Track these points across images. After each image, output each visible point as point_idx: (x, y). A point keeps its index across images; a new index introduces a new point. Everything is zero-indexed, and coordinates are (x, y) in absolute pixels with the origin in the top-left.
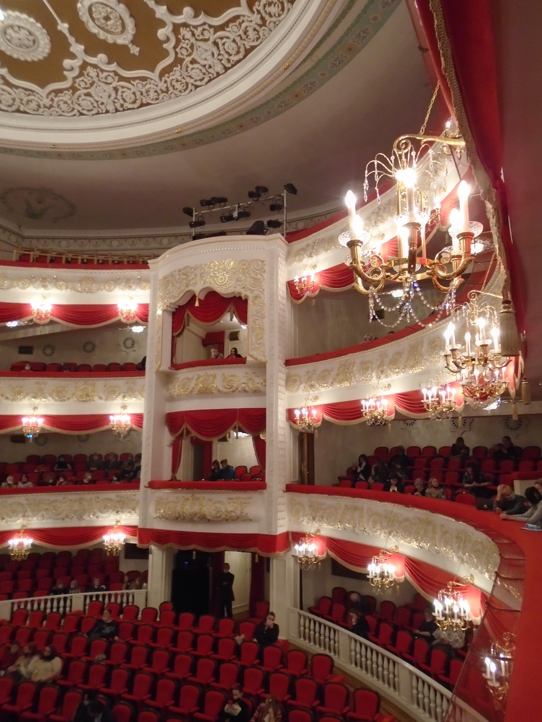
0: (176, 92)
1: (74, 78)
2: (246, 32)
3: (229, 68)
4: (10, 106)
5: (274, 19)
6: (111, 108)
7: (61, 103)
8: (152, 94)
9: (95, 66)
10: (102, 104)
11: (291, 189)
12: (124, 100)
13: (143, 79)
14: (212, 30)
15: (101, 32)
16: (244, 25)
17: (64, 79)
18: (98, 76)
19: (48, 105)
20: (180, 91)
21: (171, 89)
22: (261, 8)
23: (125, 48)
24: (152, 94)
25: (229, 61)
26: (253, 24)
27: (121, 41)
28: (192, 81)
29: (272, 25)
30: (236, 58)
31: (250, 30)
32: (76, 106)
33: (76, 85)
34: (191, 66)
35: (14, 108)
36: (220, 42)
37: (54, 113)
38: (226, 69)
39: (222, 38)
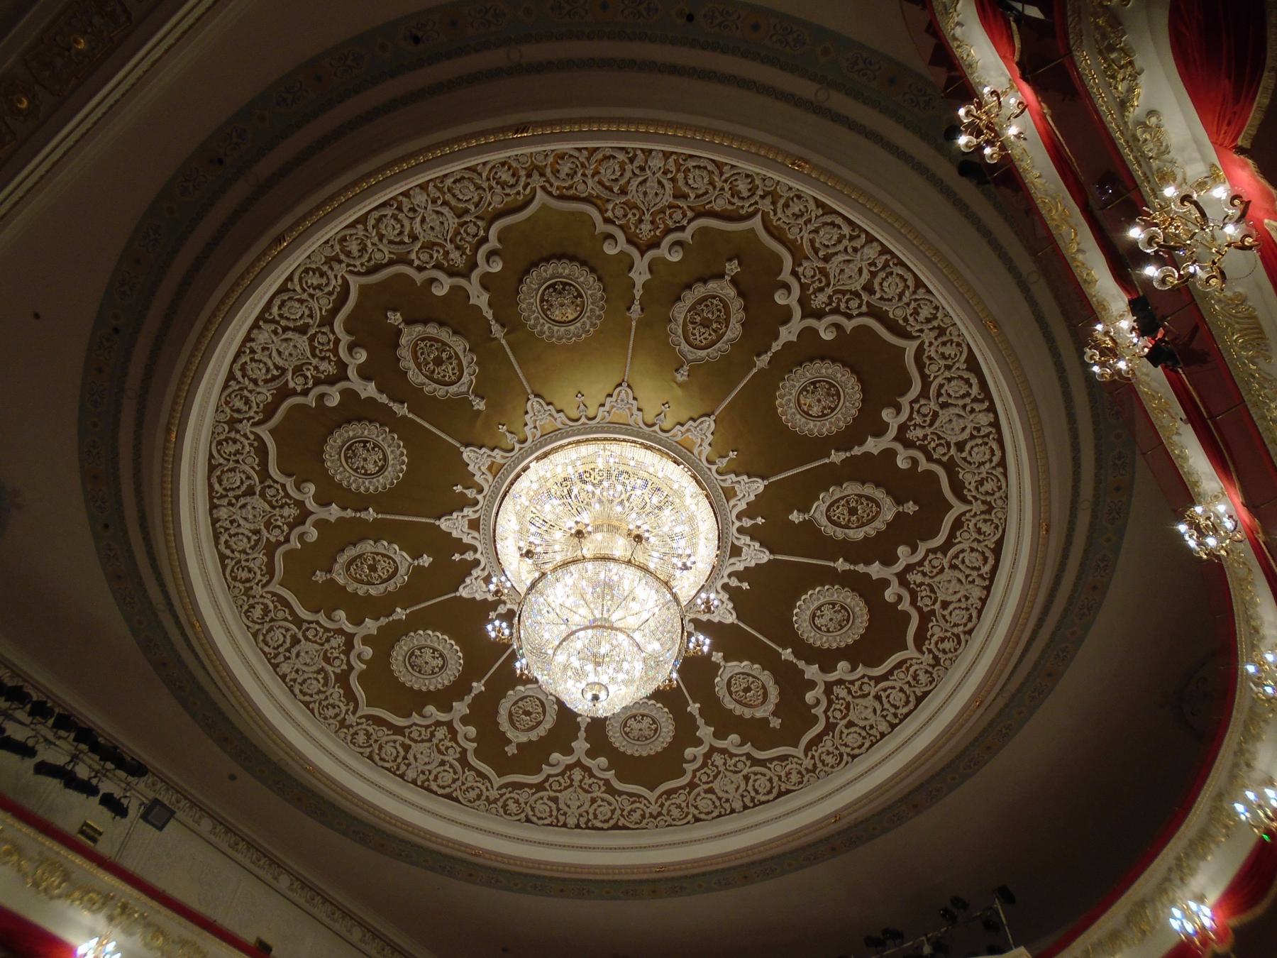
0: (826, 769)
1: (695, 772)
2: (915, 677)
3: (897, 725)
4: (606, 821)
5: (950, 655)
6: (737, 805)
7: (672, 808)
8: (794, 777)
9: (723, 751)
10: (727, 801)
11: (1006, 895)
12: (757, 792)
13: (783, 758)
14: (872, 683)
15: (738, 706)
16: (912, 670)
17: (683, 772)
18: (725, 764)
19: (655, 813)
20: (832, 767)
21: (819, 765)
22: (932, 647)
23: (765, 721)
24: (794, 777)
25: (895, 715)
26: (924, 666)
27: (759, 714)
28: (848, 750)
29: (948, 663)
30: (905, 710)
31: (921, 673)
32: (692, 810)
33: (696, 780)
34: (846, 731)
35: (612, 823)
36: (884, 695)
37: (662, 823)
38: (893, 726)
39: (885, 690)
